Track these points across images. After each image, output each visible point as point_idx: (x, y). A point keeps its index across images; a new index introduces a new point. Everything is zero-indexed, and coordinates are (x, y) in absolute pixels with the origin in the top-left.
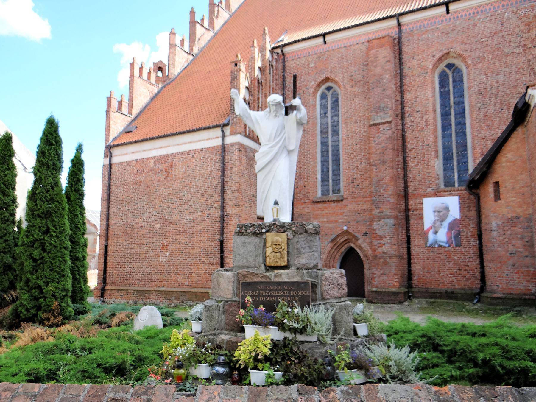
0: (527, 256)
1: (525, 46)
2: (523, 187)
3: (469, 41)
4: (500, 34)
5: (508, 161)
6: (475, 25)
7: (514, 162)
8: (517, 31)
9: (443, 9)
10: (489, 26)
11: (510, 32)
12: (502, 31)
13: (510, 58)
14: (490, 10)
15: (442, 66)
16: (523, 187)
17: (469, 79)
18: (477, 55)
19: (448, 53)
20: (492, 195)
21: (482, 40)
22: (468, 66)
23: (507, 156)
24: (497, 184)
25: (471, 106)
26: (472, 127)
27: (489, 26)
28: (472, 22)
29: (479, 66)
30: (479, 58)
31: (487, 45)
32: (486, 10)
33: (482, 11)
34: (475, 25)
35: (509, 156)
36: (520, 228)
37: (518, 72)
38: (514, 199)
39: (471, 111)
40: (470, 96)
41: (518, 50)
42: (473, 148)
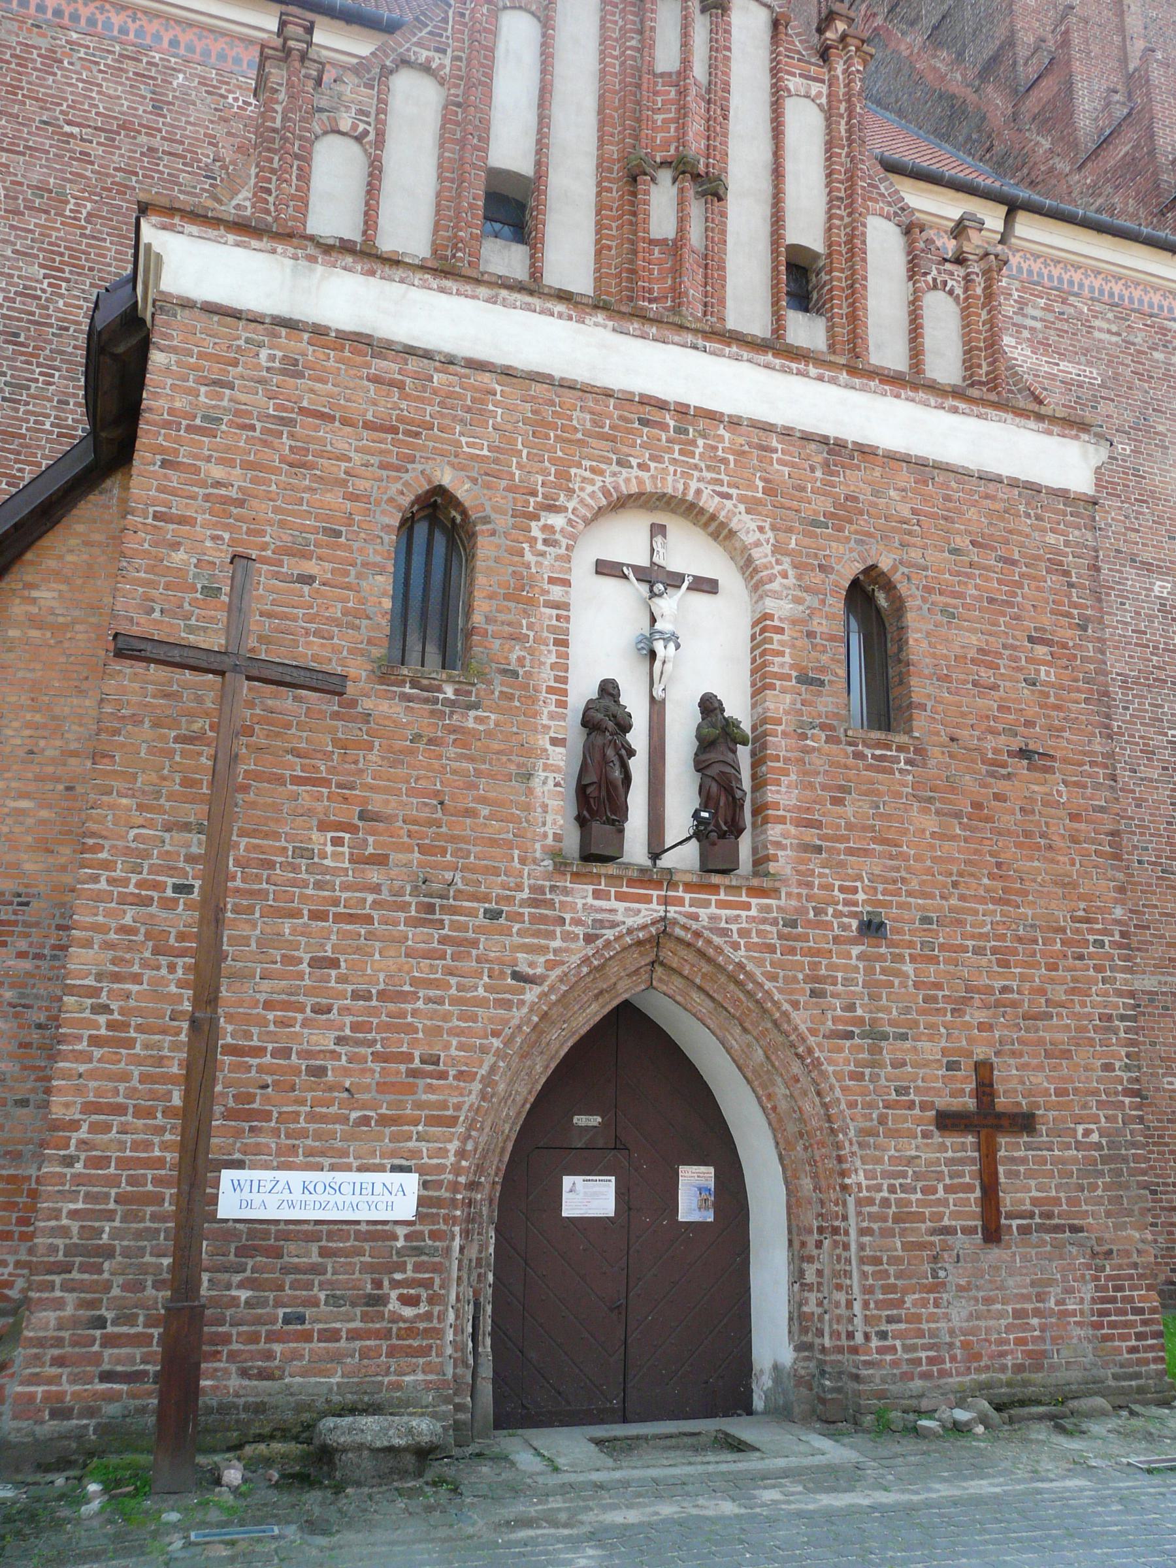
0: (23, 1103)
2: (74, 754)
3: (16, 109)
4: (143, 139)
5: (35, 622)
6: (52, 59)
7: (65, 627)
8: (206, 154)
10: (108, 88)
11: (179, 149)
12: (152, 131)
14: (123, 31)
16: (74, 754)
18: (35, 177)
21: (67, 129)
27: (108, 88)
28: (44, 43)
29: (32, 221)
30: (41, 189)
31: (85, 158)
32: (108, 25)
33: (92, 22)
35: (46, 595)
36: (21, 955)
38: (24, 804)
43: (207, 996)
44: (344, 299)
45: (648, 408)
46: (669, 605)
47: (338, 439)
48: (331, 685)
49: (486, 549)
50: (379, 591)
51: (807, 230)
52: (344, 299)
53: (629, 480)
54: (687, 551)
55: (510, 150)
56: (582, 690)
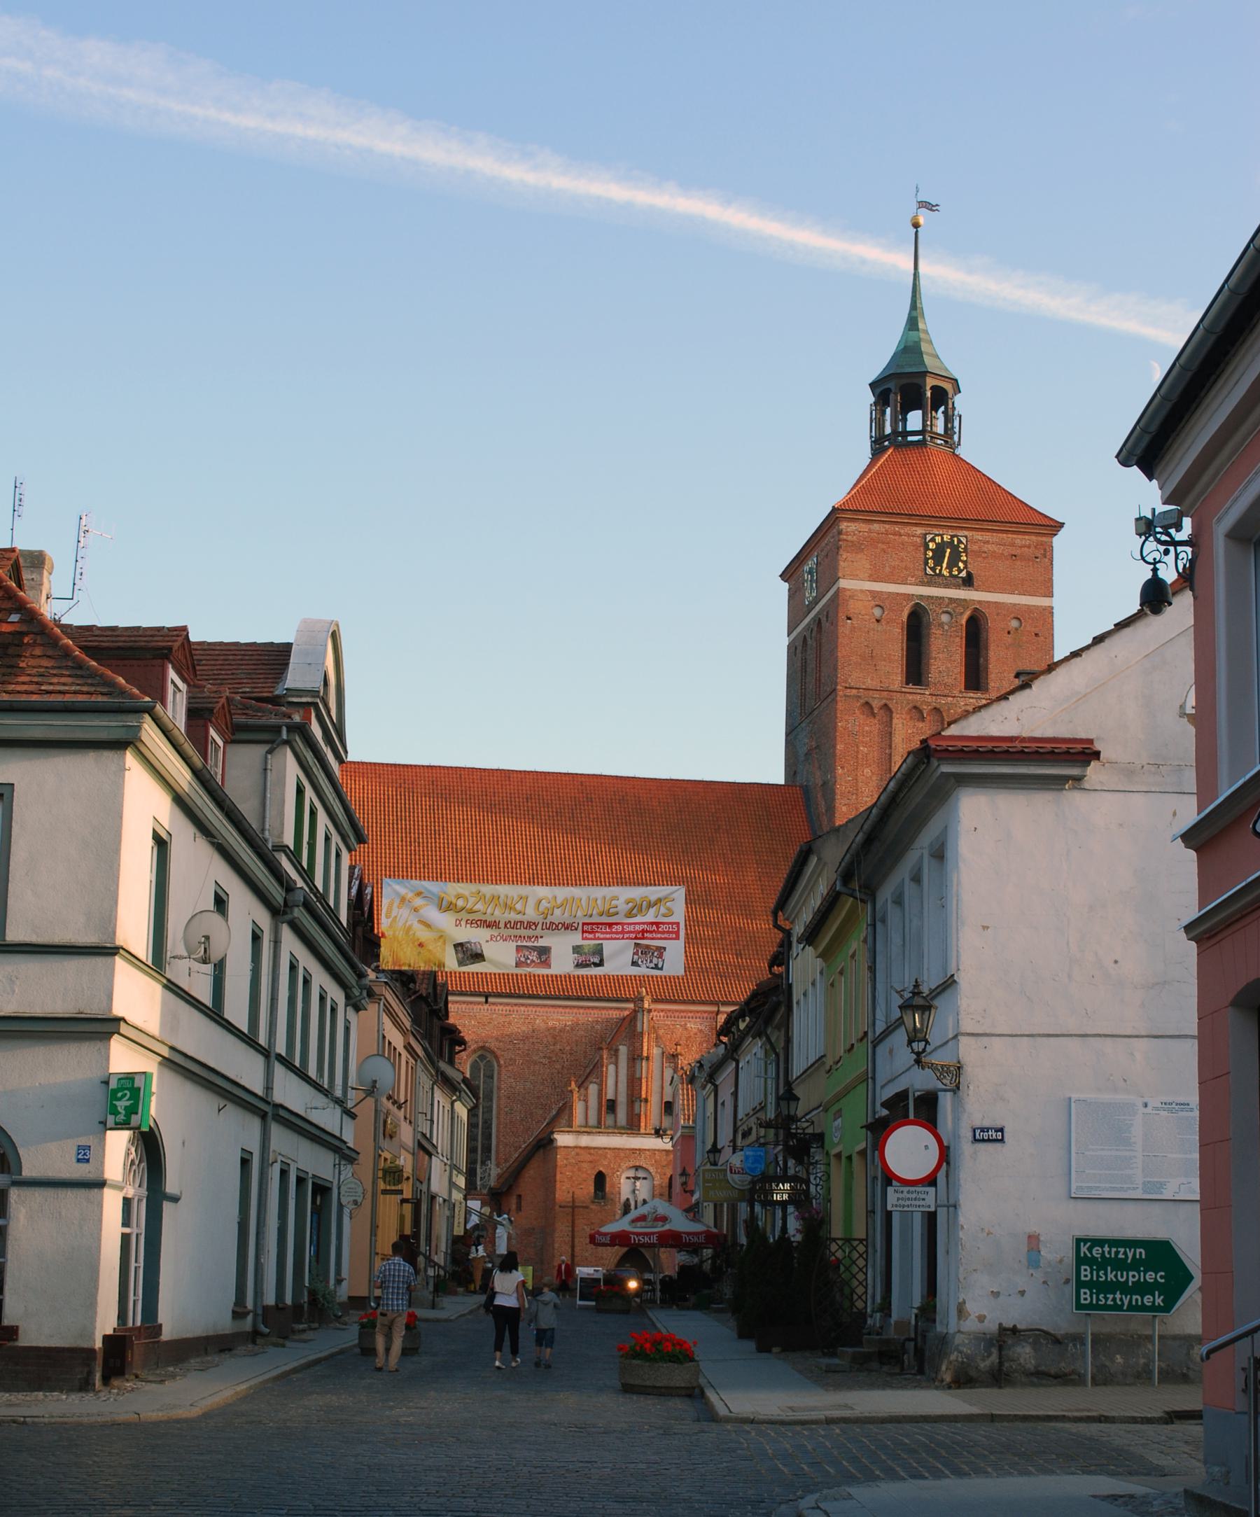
1: (550, 1058)
6: (510, 1023)
8: (545, 1040)
9: (483, 999)
13: (537, 1067)
15: (475, 1056)
17: (499, 1078)
19: (483, 1048)
20: (514, 1207)
22: (499, 1066)
23: (531, 1173)
24: (520, 1196)
25: (498, 1106)
26: (498, 1131)
34: (510, 1023)
35: (532, 1172)
37: (543, 1084)
39: (499, 1113)
40: (499, 1097)
41: (544, 1061)
42: (497, 1152)
43: (573, 1250)
44: (585, 1141)
45: (634, 1151)
46: (638, 1183)
47: (585, 1165)
48: (587, 1207)
49: (608, 1179)
50: (592, 1189)
51: (668, 1098)
52: (585, 1141)
53: (631, 1164)
54: (641, 1174)
55: (610, 1096)
56: (623, 1198)
